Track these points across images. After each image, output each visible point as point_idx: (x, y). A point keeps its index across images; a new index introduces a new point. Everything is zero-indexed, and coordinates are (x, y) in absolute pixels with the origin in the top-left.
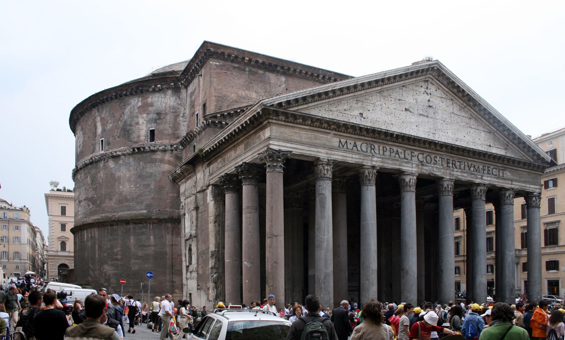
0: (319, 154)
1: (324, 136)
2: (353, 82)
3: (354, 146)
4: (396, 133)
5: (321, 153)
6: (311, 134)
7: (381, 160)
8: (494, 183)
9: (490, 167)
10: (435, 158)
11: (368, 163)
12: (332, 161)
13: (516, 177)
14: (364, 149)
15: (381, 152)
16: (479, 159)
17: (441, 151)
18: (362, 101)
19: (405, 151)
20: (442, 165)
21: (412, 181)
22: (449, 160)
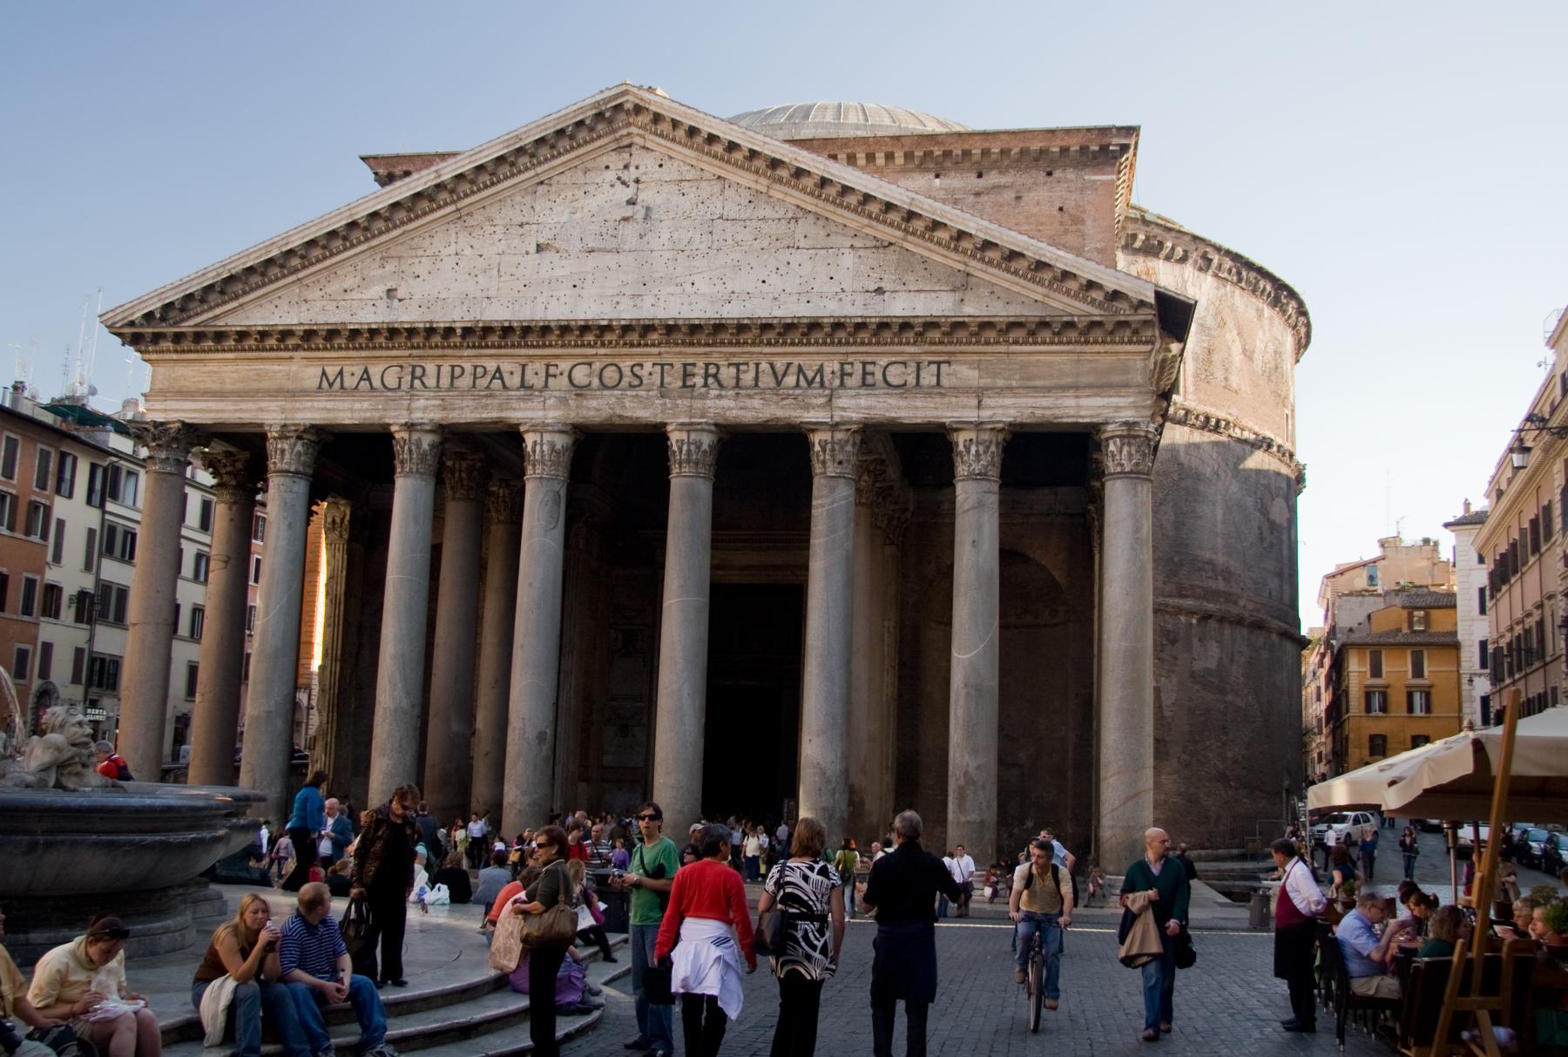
1: (281, 367)
2: (338, 218)
3: (362, 379)
5: (268, 411)
6: (249, 370)
7: (440, 402)
8: (893, 415)
9: (874, 363)
10: (636, 369)
11: (395, 417)
12: (293, 428)
13: (1008, 379)
14: (391, 381)
15: (445, 381)
16: (809, 344)
17: (646, 345)
18: (400, 258)
19: (524, 367)
20: (662, 384)
21: (538, 448)
22: (694, 365)
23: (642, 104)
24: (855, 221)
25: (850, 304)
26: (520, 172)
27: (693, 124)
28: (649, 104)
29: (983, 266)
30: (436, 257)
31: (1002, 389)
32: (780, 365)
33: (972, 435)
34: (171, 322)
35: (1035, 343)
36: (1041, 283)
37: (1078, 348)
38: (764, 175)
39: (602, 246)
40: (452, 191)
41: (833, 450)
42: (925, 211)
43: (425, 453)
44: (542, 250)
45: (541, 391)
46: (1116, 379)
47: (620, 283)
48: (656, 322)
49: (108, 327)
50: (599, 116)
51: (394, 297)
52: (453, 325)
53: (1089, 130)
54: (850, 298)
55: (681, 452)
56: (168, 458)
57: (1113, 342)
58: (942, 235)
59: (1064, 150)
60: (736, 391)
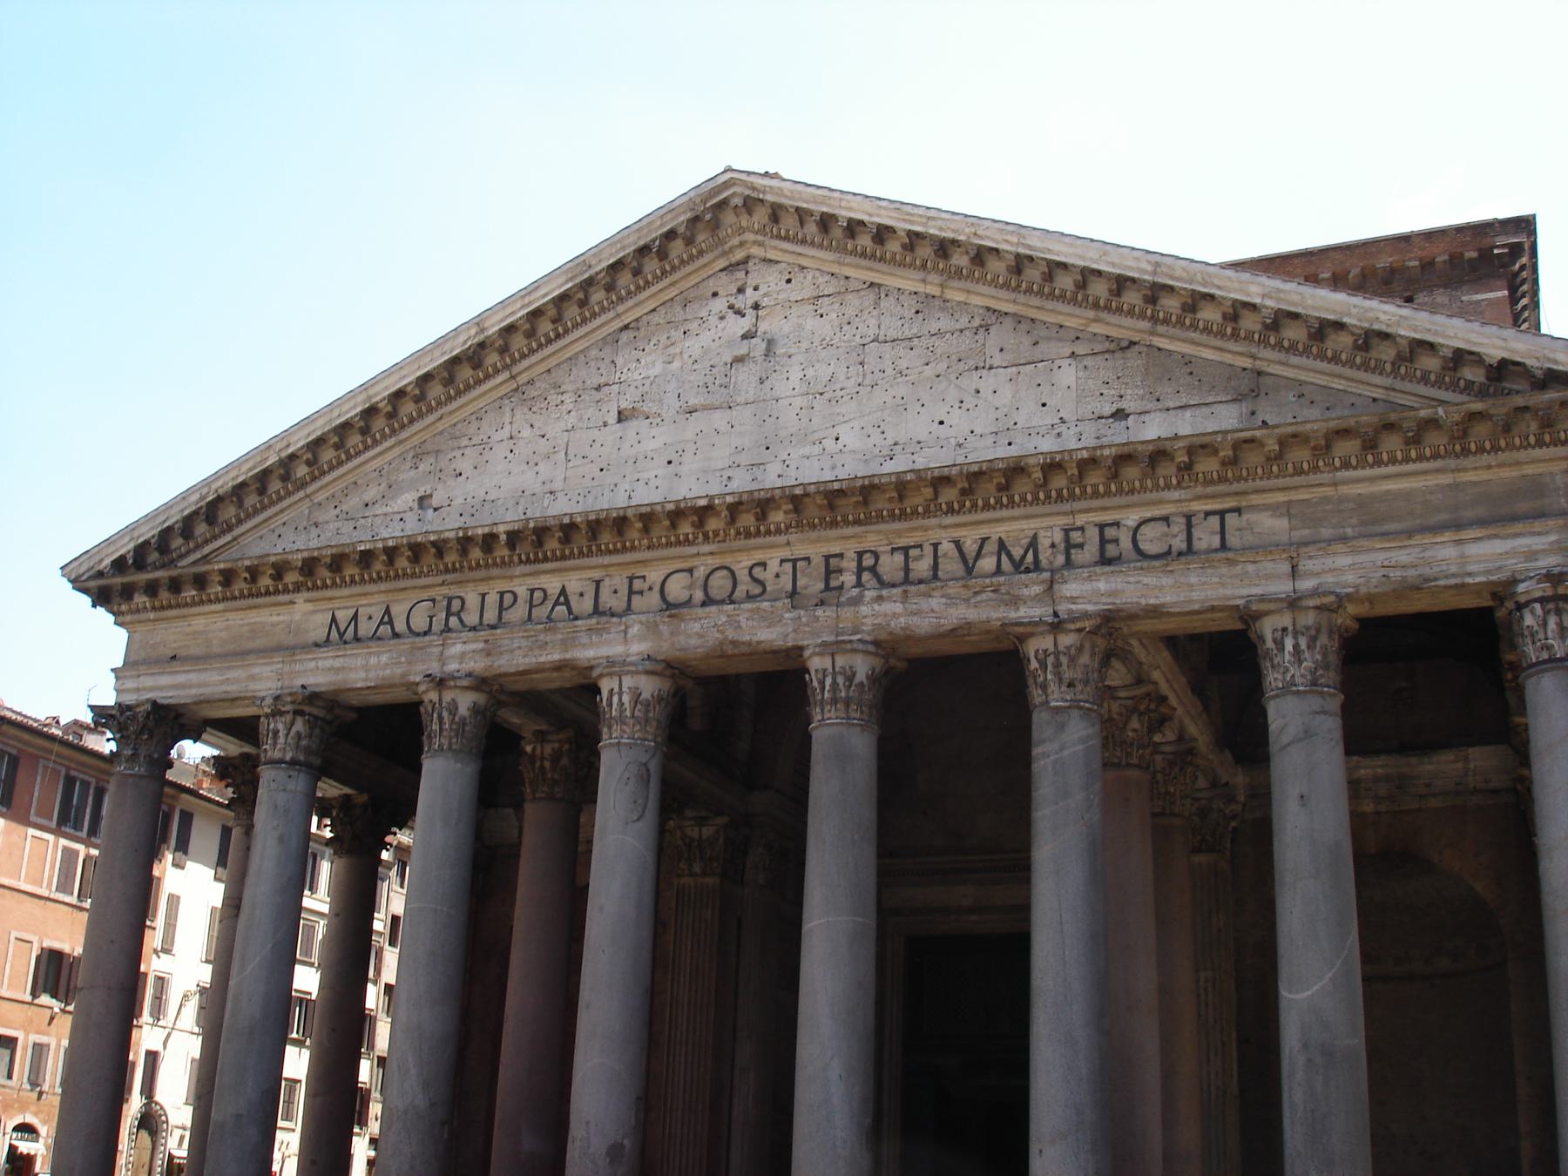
0: (252, 686)
1: (281, 618)
2: (352, 404)
3: (381, 623)
4: (501, 529)
5: (260, 679)
6: (243, 625)
8: (1152, 601)
9: (1117, 524)
10: (757, 572)
12: (289, 699)
15: (491, 616)
16: (1012, 504)
17: (768, 532)
21: (615, 699)
22: (841, 556)
23: (755, 195)
24: (1073, 317)
25: (1074, 440)
26: (594, 315)
27: (825, 209)
28: (764, 192)
29: (1282, 356)
30: (485, 445)
31: (1329, 542)
32: (970, 547)
33: (1285, 620)
34: (149, 568)
35: (1378, 463)
36: (1378, 369)
37: (1452, 463)
38: (935, 269)
39: (709, 400)
40: (504, 350)
41: (1057, 665)
42: (1177, 279)
43: (463, 720)
44: (626, 419)
45: (620, 616)
46: (1523, 507)
47: (733, 450)
48: (778, 492)
49: (71, 581)
50: (695, 220)
51: (430, 506)
52: (495, 531)
53: (1460, 230)
54: (1072, 432)
55: (823, 689)
56: (134, 756)
57: (1511, 447)
58: (1209, 314)
59: (1427, 265)
60: (904, 588)
